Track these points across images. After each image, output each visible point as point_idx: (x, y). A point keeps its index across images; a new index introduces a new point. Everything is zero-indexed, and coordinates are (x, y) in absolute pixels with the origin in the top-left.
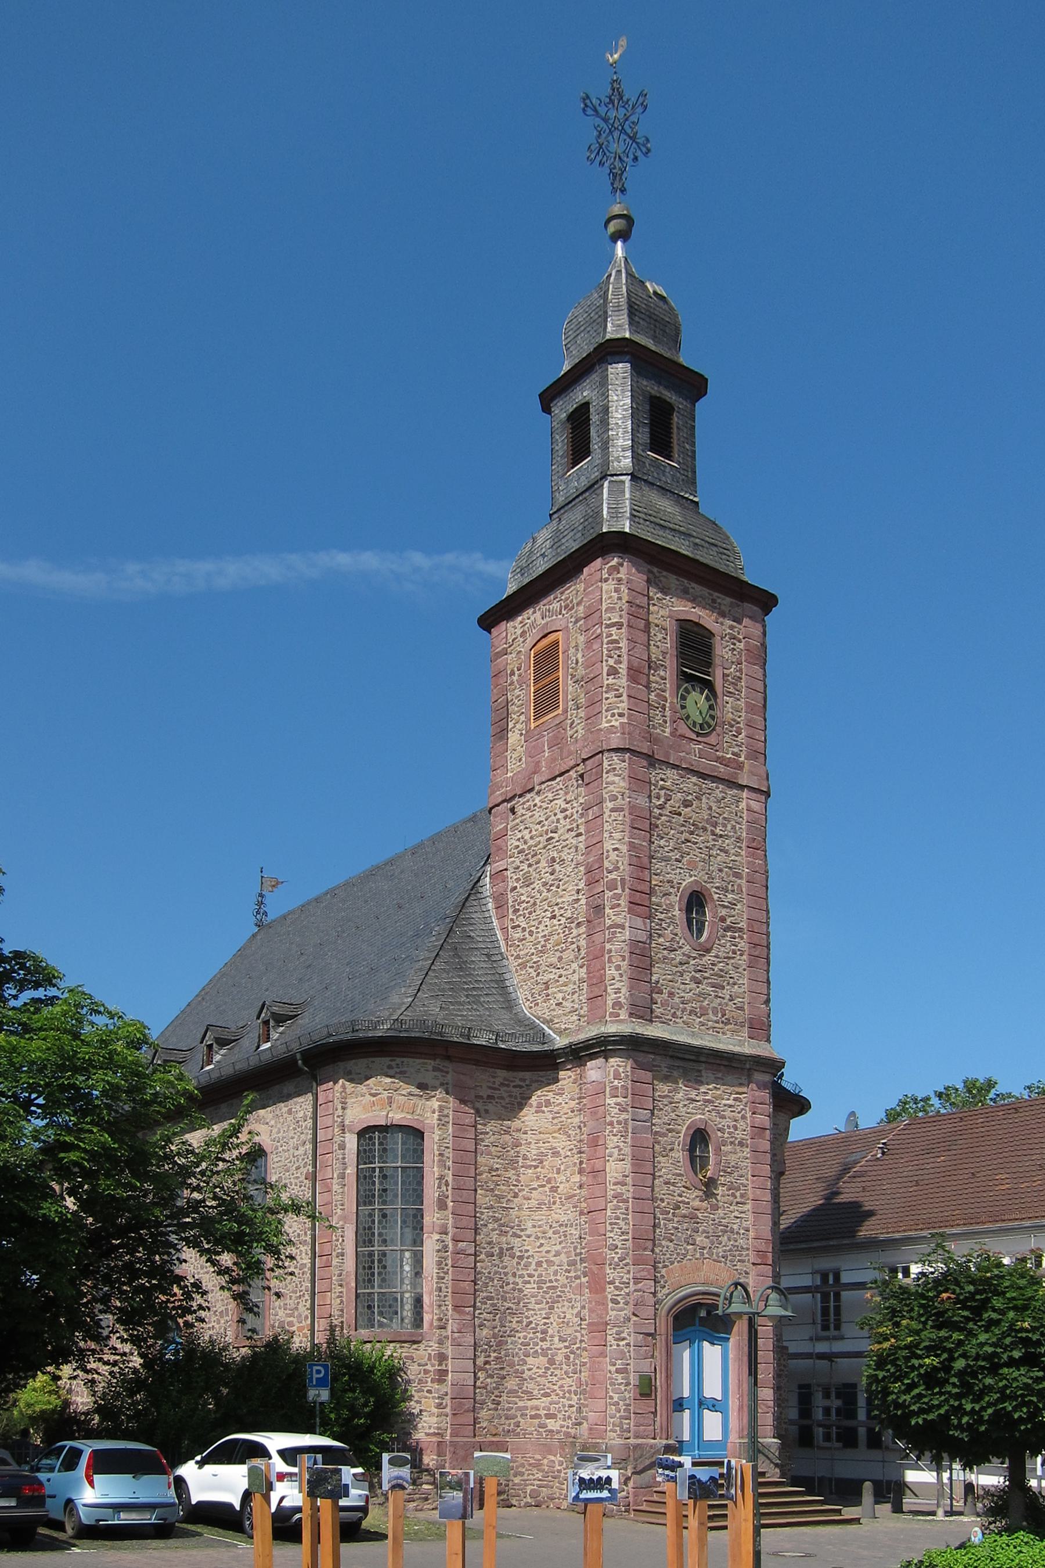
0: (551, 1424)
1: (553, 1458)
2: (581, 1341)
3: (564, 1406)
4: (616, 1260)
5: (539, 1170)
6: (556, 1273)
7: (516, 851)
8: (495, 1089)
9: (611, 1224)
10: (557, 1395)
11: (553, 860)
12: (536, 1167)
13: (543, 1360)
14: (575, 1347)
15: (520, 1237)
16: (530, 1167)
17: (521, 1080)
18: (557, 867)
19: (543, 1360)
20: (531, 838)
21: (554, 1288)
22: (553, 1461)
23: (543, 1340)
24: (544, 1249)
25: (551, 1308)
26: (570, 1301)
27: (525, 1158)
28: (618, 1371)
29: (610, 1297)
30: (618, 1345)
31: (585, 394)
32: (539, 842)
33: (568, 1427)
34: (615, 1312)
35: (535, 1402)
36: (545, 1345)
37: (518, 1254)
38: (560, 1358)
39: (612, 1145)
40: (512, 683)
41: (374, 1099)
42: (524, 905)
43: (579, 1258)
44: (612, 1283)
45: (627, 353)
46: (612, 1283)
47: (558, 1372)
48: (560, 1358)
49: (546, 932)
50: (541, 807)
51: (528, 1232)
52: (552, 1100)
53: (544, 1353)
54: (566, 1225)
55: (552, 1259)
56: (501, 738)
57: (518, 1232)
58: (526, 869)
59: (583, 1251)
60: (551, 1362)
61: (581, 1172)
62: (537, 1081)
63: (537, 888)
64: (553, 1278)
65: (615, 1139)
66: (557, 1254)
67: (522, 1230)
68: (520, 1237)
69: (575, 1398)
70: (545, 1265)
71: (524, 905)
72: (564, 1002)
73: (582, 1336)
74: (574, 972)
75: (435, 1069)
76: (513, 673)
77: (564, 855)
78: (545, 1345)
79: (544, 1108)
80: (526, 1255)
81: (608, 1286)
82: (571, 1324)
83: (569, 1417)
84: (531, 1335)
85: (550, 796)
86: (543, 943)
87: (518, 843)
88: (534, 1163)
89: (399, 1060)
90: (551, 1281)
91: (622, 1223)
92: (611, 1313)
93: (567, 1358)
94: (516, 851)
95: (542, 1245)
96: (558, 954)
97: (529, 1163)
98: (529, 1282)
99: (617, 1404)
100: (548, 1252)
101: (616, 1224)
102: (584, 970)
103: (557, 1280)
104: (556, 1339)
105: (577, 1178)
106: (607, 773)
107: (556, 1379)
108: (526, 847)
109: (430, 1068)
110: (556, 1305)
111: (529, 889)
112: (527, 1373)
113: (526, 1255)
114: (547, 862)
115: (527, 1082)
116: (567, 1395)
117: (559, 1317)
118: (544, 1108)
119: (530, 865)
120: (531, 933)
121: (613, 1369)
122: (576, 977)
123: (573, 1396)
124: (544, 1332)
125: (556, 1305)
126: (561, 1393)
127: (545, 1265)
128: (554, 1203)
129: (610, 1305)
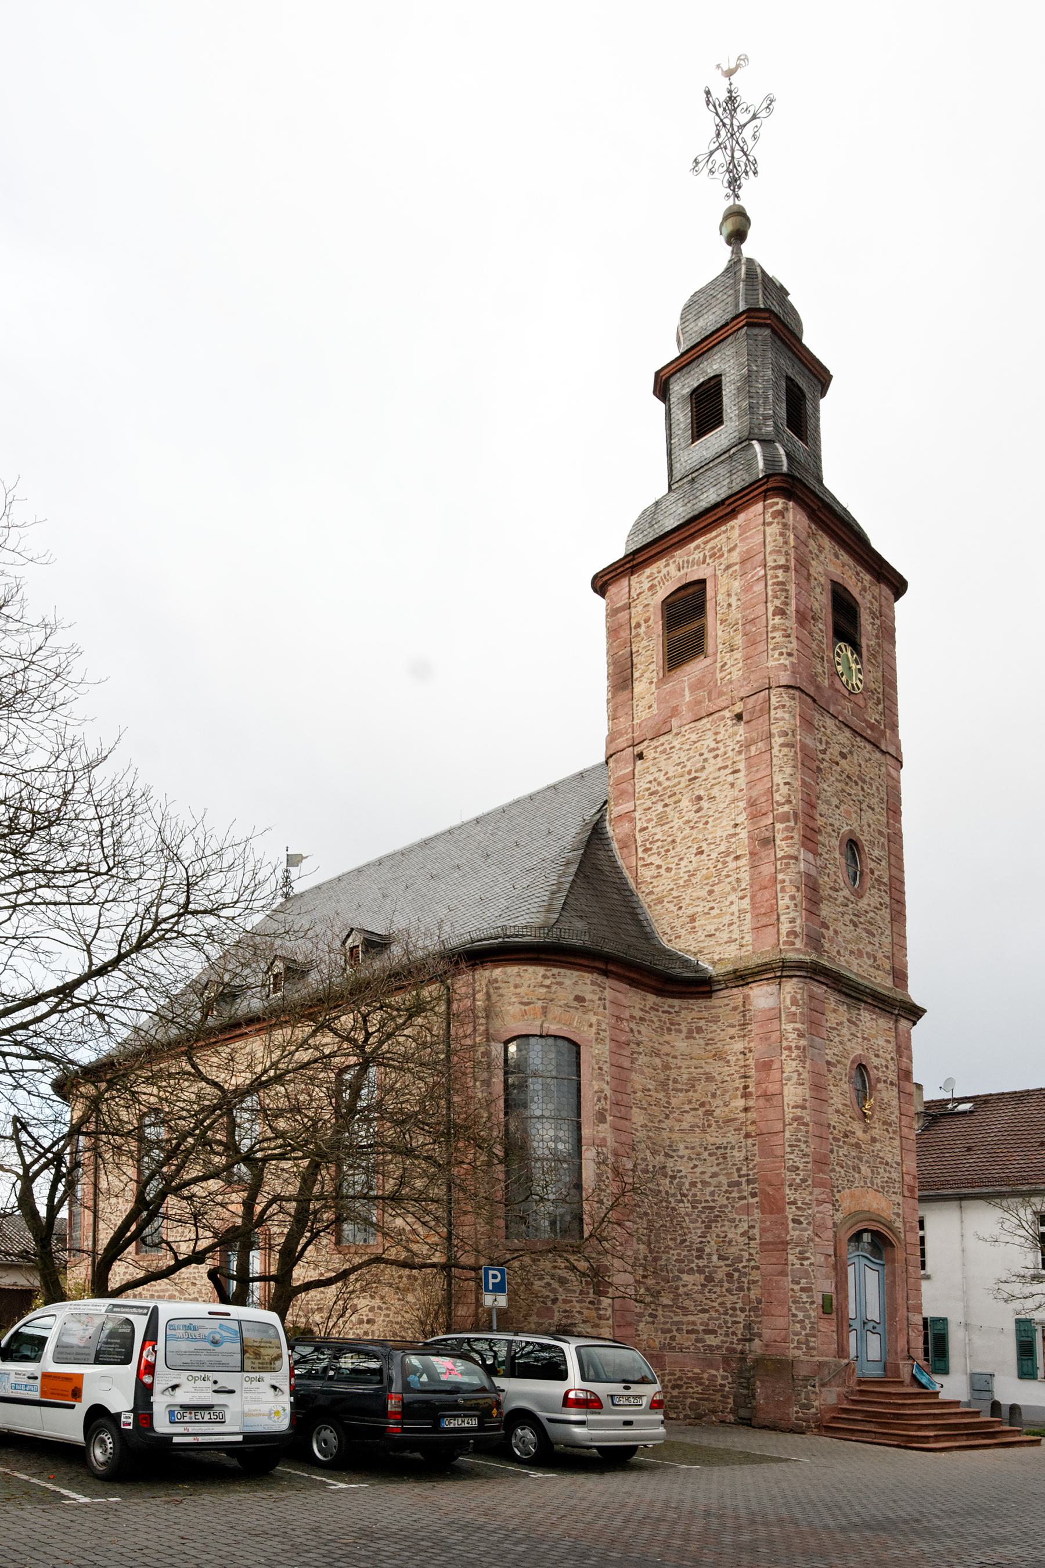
0: (712, 1340)
1: (714, 1372)
2: (749, 1260)
3: (726, 1322)
4: (798, 1181)
5: (691, 1093)
6: (712, 1194)
7: (647, 793)
8: (647, 1012)
9: (790, 1146)
10: (717, 1311)
11: (699, 798)
12: (687, 1091)
13: (700, 1278)
14: (741, 1265)
15: (672, 1157)
16: (681, 1090)
17: (670, 1006)
18: (704, 804)
19: (700, 1278)
20: (668, 779)
21: (712, 1208)
22: (716, 1376)
23: (699, 1257)
24: (698, 1170)
25: (708, 1227)
26: (733, 1220)
27: (675, 1081)
28: (802, 1290)
29: (790, 1217)
30: (802, 1265)
31: (715, 367)
32: (679, 783)
33: (732, 1343)
34: (797, 1233)
35: (691, 1318)
36: (701, 1263)
37: (670, 1173)
38: (720, 1275)
39: (790, 1070)
40: (637, 635)
41: (526, 1008)
42: (659, 844)
43: (744, 1179)
44: (794, 1203)
45: (767, 326)
46: (794, 1203)
47: (717, 1289)
48: (720, 1275)
49: (691, 868)
50: (680, 749)
51: (680, 1153)
52: (704, 1027)
53: (700, 1270)
54: (726, 1148)
55: (708, 1180)
56: (624, 688)
57: (671, 1153)
58: (661, 809)
59: (751, 1172)
60: (709, 1279)
61: (746, 1095)
62: (687, 1009)
63: (677, 827)
64: (709, 1199)
65: (794, 1063)
66: (714, 1175)
67: (674, 1151)
68: (672, 1157)
69: (743, 1315)
70: (699, 1186)
71: (659, 844)
72: (717, 933)
73: (750, 1254)
74: (732, 903)
75: (593, 983)
76: (638, 625)
77: (715, 792)
78: (701, 1263)
79: (695, 1035)
80: (679, 1175)
81: (787, 1206)
82: (734, 1243)
83: (734, 1333)
84: (686, 1253)
85: (694, 737)
86: (686, 878)
87: (648, 785)
88: (685, 1087)
89: (555, 971)
90: (707, 1201)
91: (803, 1146)
92: (792, 1233)
93: (729, 1275)
94: (647, 793)
95: (695, 1166)
96: (708, 888)
97: (679, 1086)
98: (682, 1201)
99: (802, 1322)
100: (703, 1173)
101: (796, 1146)
102: (747, 900)
103: (713, 1201)
104: (715, 1258)
105: (741, 1103)
106: (775, 709)
107: (714, 1296)
108: (660, 788)
109: (589, 982)
110: (713, 1225)
111: (665, 827)
112: (681, 1290)
113: (679, 1175)
114: (691, 800)
115: (677, 1009)
116: (730, 1312)
117: (718, 1236)
118: (695, 1035)
119: (666, 805)
120: (668, 870)
121: (797, 1287)
122: (734, 908)
123: (738, 1312)
124: (701, 1250)
125: (713, 1225)
126: (721, 1310)
127: (699, 1186)
128: (709, 1126)
129: (791, 1225)
